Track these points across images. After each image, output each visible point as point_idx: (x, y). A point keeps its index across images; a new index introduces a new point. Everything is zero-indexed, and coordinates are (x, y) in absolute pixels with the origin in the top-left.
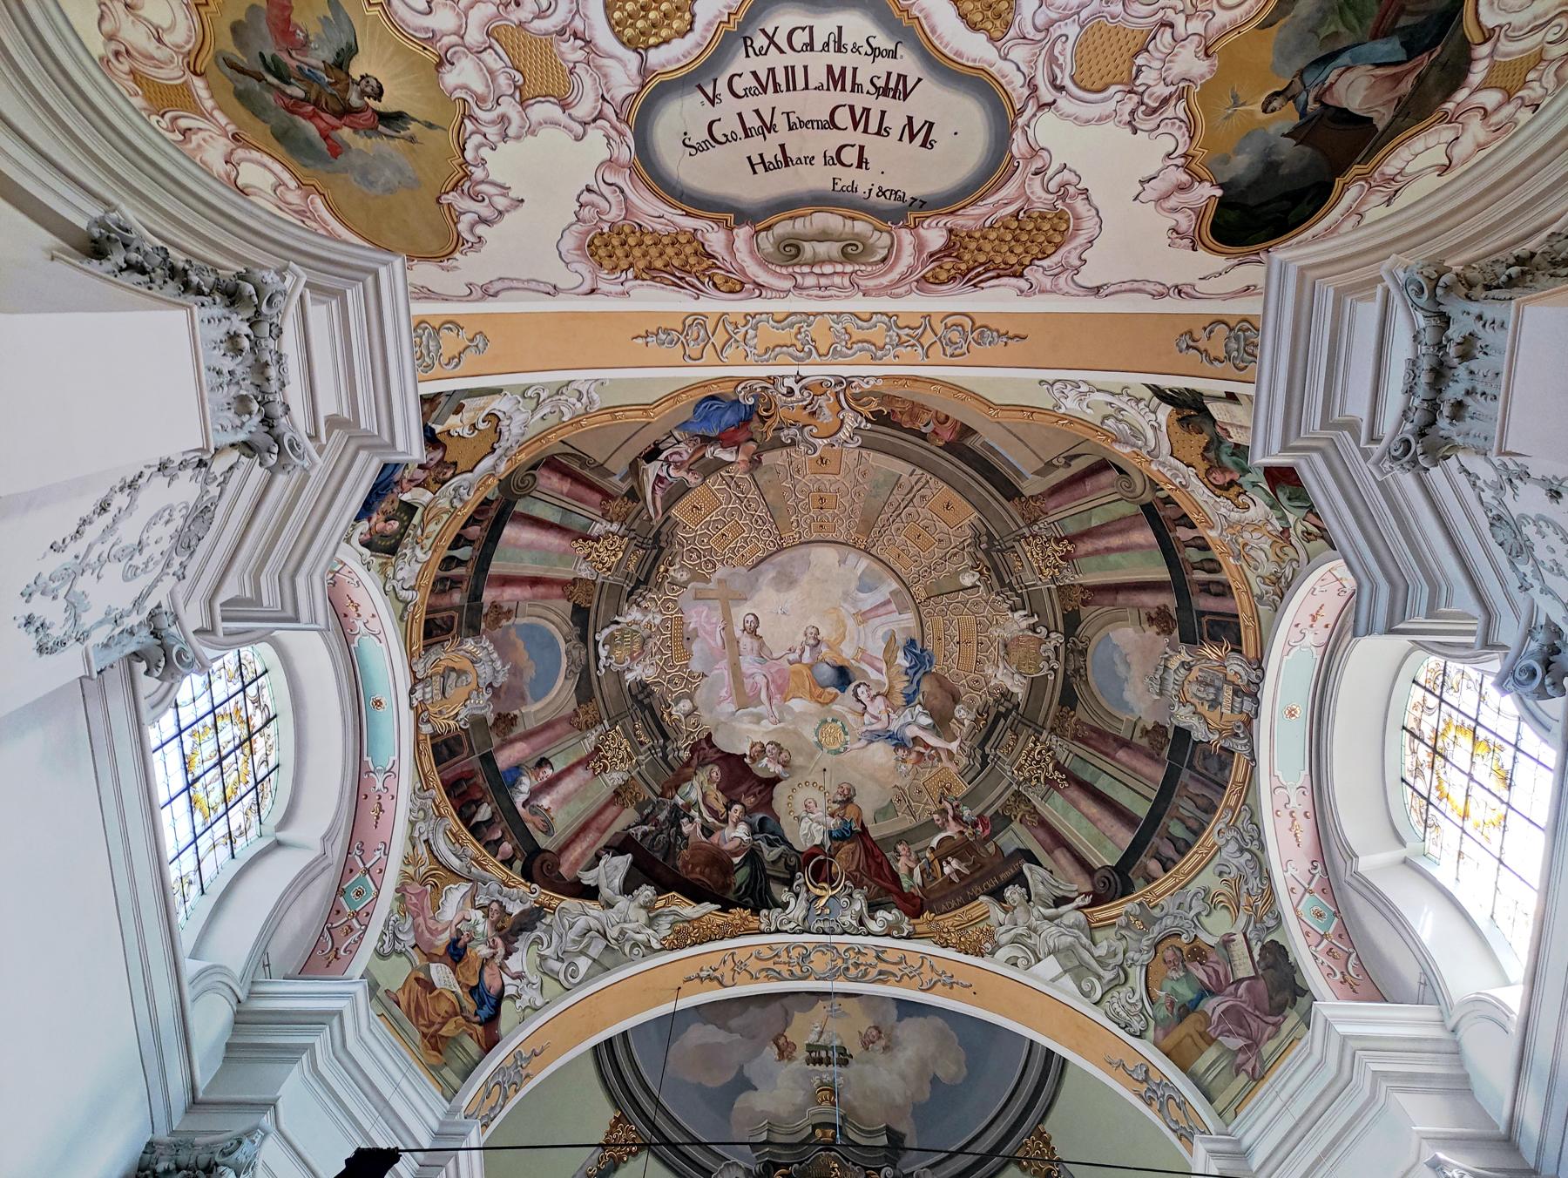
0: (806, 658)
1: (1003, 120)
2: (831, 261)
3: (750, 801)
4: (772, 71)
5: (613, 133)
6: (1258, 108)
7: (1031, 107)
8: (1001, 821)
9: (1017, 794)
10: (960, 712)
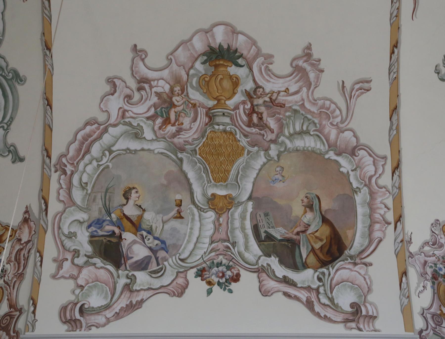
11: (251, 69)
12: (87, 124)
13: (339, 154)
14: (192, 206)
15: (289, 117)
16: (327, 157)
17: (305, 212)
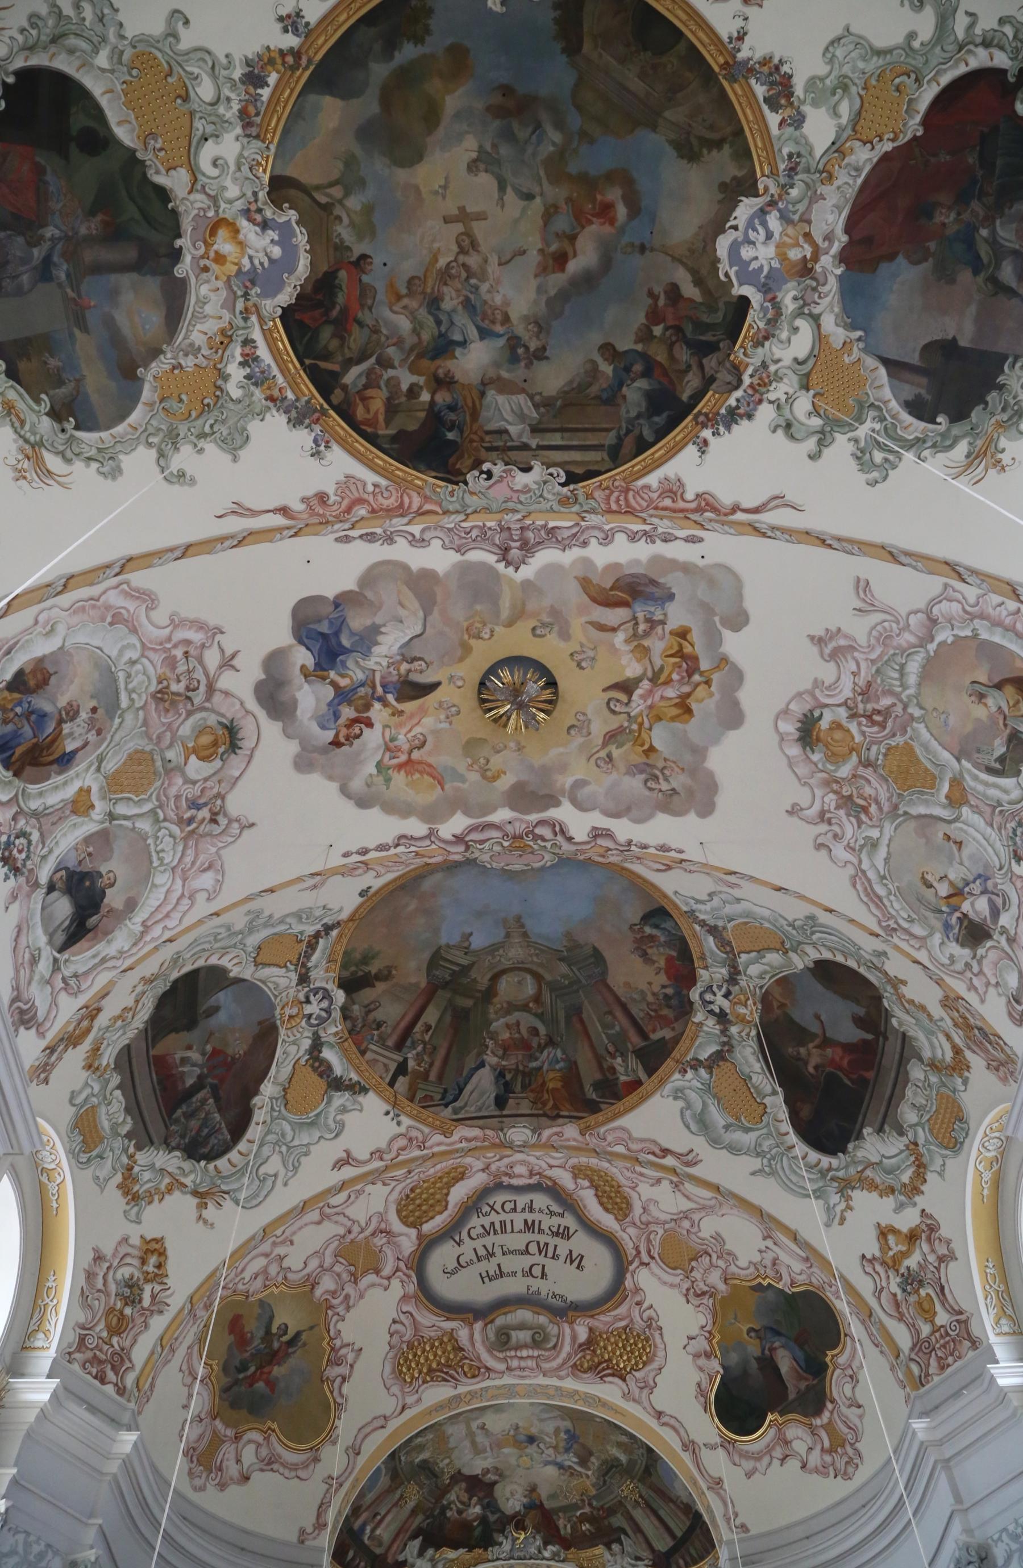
0: (512, 1433)
1: (621, 1266)
2: (526, 1346)
3: (481, 1494)
4: (493, 1224)
5: (405, 1278)
6: (745, 1329)
7: (636, 1264)
8: (611, 1511)
9: (620, 1502)
10: (593, 1459)
11: (827, 706)
12: (854, 885)
13: (932, 640)
14: (953, 826)
15: (883, 681)
16: (932, 654)
17: (985, 705)
